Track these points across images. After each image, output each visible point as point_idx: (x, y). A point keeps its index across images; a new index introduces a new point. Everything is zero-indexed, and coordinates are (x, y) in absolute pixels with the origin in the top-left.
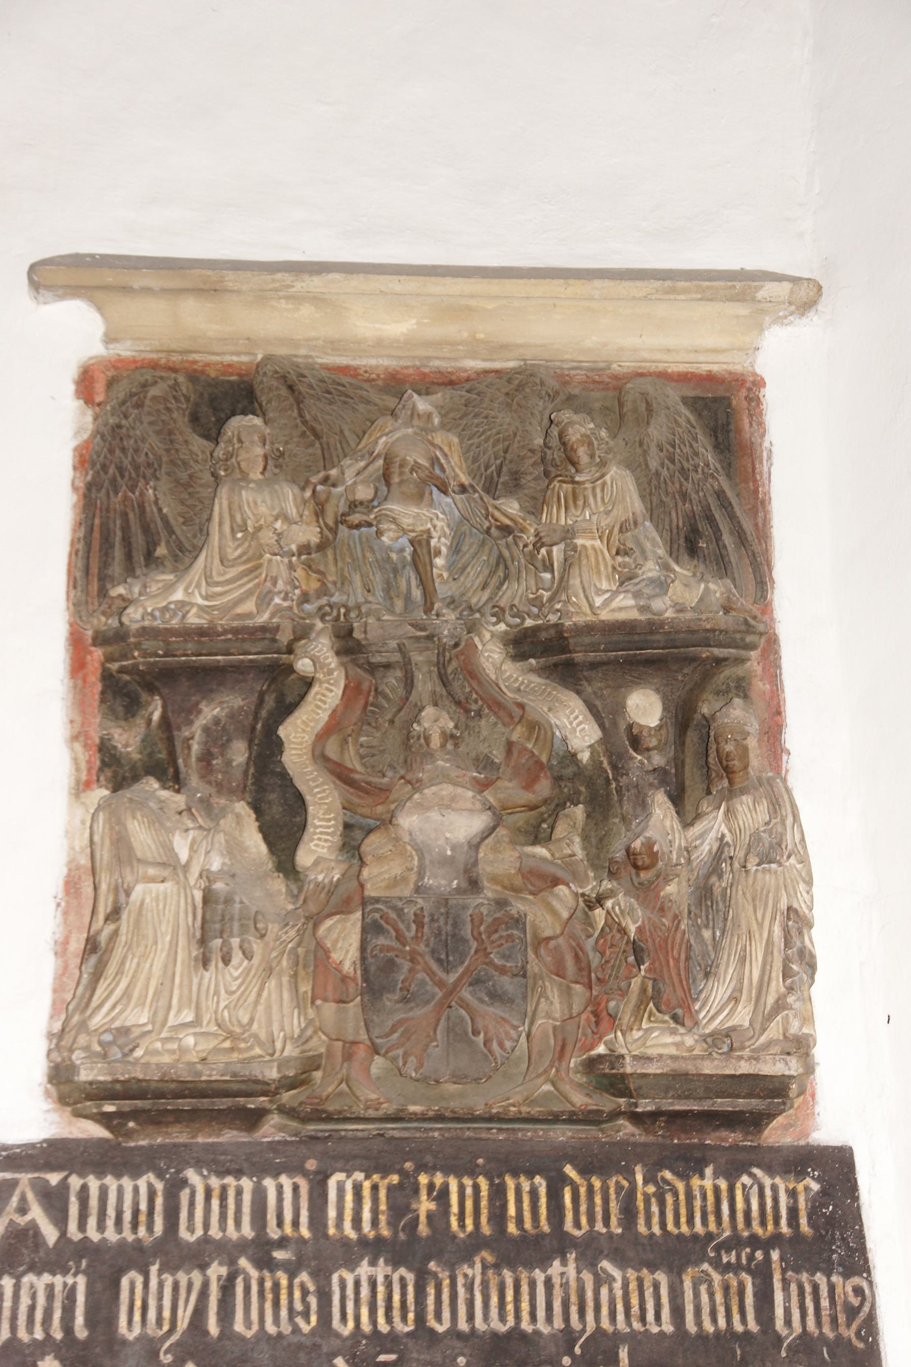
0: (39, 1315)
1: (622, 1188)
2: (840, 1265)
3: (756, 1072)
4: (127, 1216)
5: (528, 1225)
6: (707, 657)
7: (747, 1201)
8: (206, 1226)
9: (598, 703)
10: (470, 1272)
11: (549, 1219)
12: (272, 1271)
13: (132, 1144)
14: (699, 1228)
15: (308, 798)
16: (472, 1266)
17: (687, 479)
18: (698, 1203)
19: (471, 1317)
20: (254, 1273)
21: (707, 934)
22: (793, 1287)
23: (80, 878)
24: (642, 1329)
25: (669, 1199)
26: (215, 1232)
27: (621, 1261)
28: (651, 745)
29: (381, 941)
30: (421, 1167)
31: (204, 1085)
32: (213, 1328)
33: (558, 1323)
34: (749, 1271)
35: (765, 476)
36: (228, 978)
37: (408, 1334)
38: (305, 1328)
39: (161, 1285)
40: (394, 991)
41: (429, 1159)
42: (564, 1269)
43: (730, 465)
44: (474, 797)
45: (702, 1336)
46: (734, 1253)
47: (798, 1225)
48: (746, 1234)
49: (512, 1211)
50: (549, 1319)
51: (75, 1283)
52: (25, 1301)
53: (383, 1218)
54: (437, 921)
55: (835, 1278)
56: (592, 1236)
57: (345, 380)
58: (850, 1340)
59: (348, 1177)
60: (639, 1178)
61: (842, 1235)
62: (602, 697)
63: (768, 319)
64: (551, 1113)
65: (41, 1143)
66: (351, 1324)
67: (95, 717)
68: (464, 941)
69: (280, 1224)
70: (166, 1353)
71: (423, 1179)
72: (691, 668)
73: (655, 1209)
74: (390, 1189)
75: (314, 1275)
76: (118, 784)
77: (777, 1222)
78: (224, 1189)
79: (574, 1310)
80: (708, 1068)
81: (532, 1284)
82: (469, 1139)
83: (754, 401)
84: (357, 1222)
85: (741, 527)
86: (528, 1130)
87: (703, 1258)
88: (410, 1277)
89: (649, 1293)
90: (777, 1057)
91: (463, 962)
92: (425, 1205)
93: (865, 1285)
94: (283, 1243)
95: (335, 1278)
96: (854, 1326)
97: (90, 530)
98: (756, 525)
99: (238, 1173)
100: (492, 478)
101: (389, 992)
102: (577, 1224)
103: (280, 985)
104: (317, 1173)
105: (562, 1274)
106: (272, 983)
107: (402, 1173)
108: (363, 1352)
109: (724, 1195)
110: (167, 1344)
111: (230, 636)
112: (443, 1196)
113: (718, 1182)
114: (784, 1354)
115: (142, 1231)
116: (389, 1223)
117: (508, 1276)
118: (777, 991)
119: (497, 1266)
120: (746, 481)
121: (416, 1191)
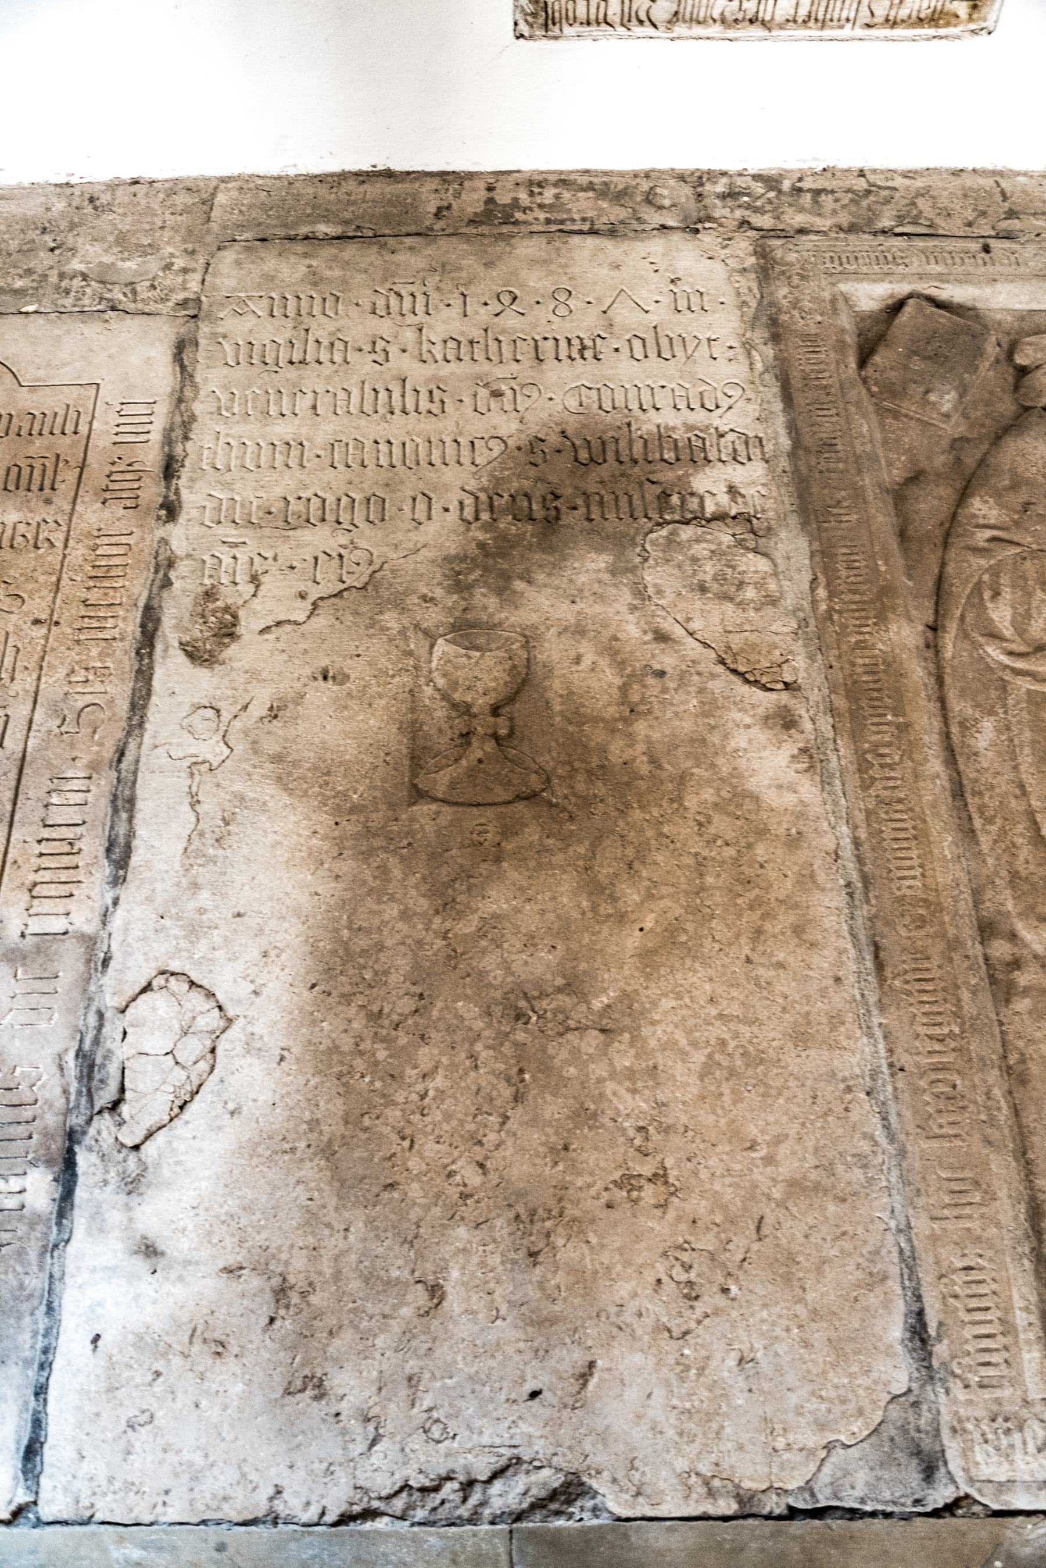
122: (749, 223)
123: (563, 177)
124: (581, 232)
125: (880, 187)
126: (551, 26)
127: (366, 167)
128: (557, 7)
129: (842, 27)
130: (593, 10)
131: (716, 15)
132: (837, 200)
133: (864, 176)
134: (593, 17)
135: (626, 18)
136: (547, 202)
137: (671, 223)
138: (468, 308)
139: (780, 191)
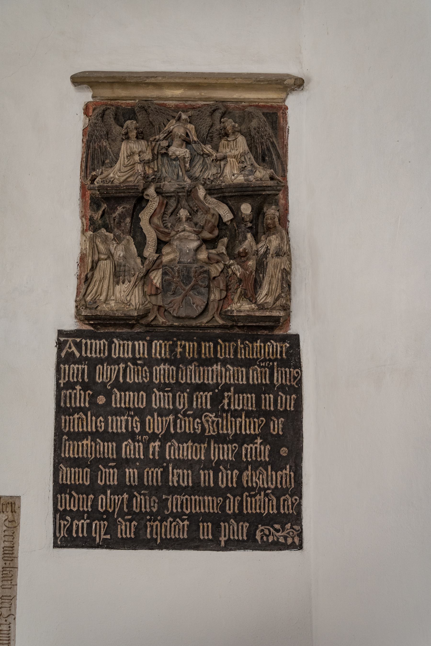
0: (75, 375)
1: (234, 345)
2: (293, 366)
3: (271, 315)
4: (98, 351)
5: (207, 355)
6: (265, 194)
7: (269, 349)
8: (119, 354)
9: (233, 207)
10: (191, 368)
11: (213, 354)
12: (137, 366)
13: (99, 332)
14: (255, 356)
15: (147, 236)
16: (191, 366)
17: (263, 139)
18: (255, 350)
19: (191, 379)
20: (132, 367)
21: (261, 275)
22: (280, 372)
23: (84, 257)
24: (238, 383)
25: (247, 349)
27: (233, 365)
28: (247, 220)
29: (167, 277)
30: (178, 339)
31: (117, 317)
32: (121, 380)
33: (215, 381)
34: (268, 367)
35: (287, 137)
36: (124, 287)
37: (174, 383)
38: (146, 381)
39: (107, 369)
40: (170, 292)
41: (180, 337)
42: (217, 367)
43: (276, 133)
44: (194, 236)
45: (254, 384)
46: (264, 363)
47: (282, 355)
48: (268, 358)
49: (203, 351)
50: (212, 380)
52: (71, 371)
53: (167, 353)
54: (183, 271)
55: (291, 370)
56: (225, 358)
57: (162, 108)
58: (294, 385)
59: (158, 342)
60: (239, 343)
61: (294, 358)
62: (234, 206)
63: (289, 89)
64: (214, 326)
65: (74, 330)
66: (158, 381)
67: (88, 210)
68: (191, 277)
69: (139, 354)
70: (109, 386)
71: (179, 343)
72: (260, 197)
73: (243, 351)
74: (169, 345)
75: (148, 367)
76: (95, 230)
77: (277, 355)
78: (124, 344)
79: (219, 378)
80: (258, 314)
81: (208, 371)
82: (192, 332)
83: (285, 114)
84: (160, 354)
85: (278, 153)
86: (208, 330)
87: (256, 364)
88: (175, 369)
89: (240, 374)
90: (277, 311)
91: (190, 284)
92: (179, 350)
93: (299, 371)
94: (140, 359)
95: (154, 368)
96: (295, 382)
97: (87, 155)
98: (283, 152)
99: (128, 340)
100: (205, 138)
101: (169, 291)
102: (221, 355)
103: (139, 289)
104: (149, 340)
105: (216, 368)
106: (136, 289)
107: (173, 341)
108: (161, 387)
109: (263, 347)
110: (109, 384)
111: (125, 188)
112: (185, 346)
113: (261, 344)
114: (276, 389)
115: (102, 355)
116: (169, 354)
117: (202, 369)
118: (279, 292)
119: (199, 366)
120: (281, 139)
121: (177, 346)
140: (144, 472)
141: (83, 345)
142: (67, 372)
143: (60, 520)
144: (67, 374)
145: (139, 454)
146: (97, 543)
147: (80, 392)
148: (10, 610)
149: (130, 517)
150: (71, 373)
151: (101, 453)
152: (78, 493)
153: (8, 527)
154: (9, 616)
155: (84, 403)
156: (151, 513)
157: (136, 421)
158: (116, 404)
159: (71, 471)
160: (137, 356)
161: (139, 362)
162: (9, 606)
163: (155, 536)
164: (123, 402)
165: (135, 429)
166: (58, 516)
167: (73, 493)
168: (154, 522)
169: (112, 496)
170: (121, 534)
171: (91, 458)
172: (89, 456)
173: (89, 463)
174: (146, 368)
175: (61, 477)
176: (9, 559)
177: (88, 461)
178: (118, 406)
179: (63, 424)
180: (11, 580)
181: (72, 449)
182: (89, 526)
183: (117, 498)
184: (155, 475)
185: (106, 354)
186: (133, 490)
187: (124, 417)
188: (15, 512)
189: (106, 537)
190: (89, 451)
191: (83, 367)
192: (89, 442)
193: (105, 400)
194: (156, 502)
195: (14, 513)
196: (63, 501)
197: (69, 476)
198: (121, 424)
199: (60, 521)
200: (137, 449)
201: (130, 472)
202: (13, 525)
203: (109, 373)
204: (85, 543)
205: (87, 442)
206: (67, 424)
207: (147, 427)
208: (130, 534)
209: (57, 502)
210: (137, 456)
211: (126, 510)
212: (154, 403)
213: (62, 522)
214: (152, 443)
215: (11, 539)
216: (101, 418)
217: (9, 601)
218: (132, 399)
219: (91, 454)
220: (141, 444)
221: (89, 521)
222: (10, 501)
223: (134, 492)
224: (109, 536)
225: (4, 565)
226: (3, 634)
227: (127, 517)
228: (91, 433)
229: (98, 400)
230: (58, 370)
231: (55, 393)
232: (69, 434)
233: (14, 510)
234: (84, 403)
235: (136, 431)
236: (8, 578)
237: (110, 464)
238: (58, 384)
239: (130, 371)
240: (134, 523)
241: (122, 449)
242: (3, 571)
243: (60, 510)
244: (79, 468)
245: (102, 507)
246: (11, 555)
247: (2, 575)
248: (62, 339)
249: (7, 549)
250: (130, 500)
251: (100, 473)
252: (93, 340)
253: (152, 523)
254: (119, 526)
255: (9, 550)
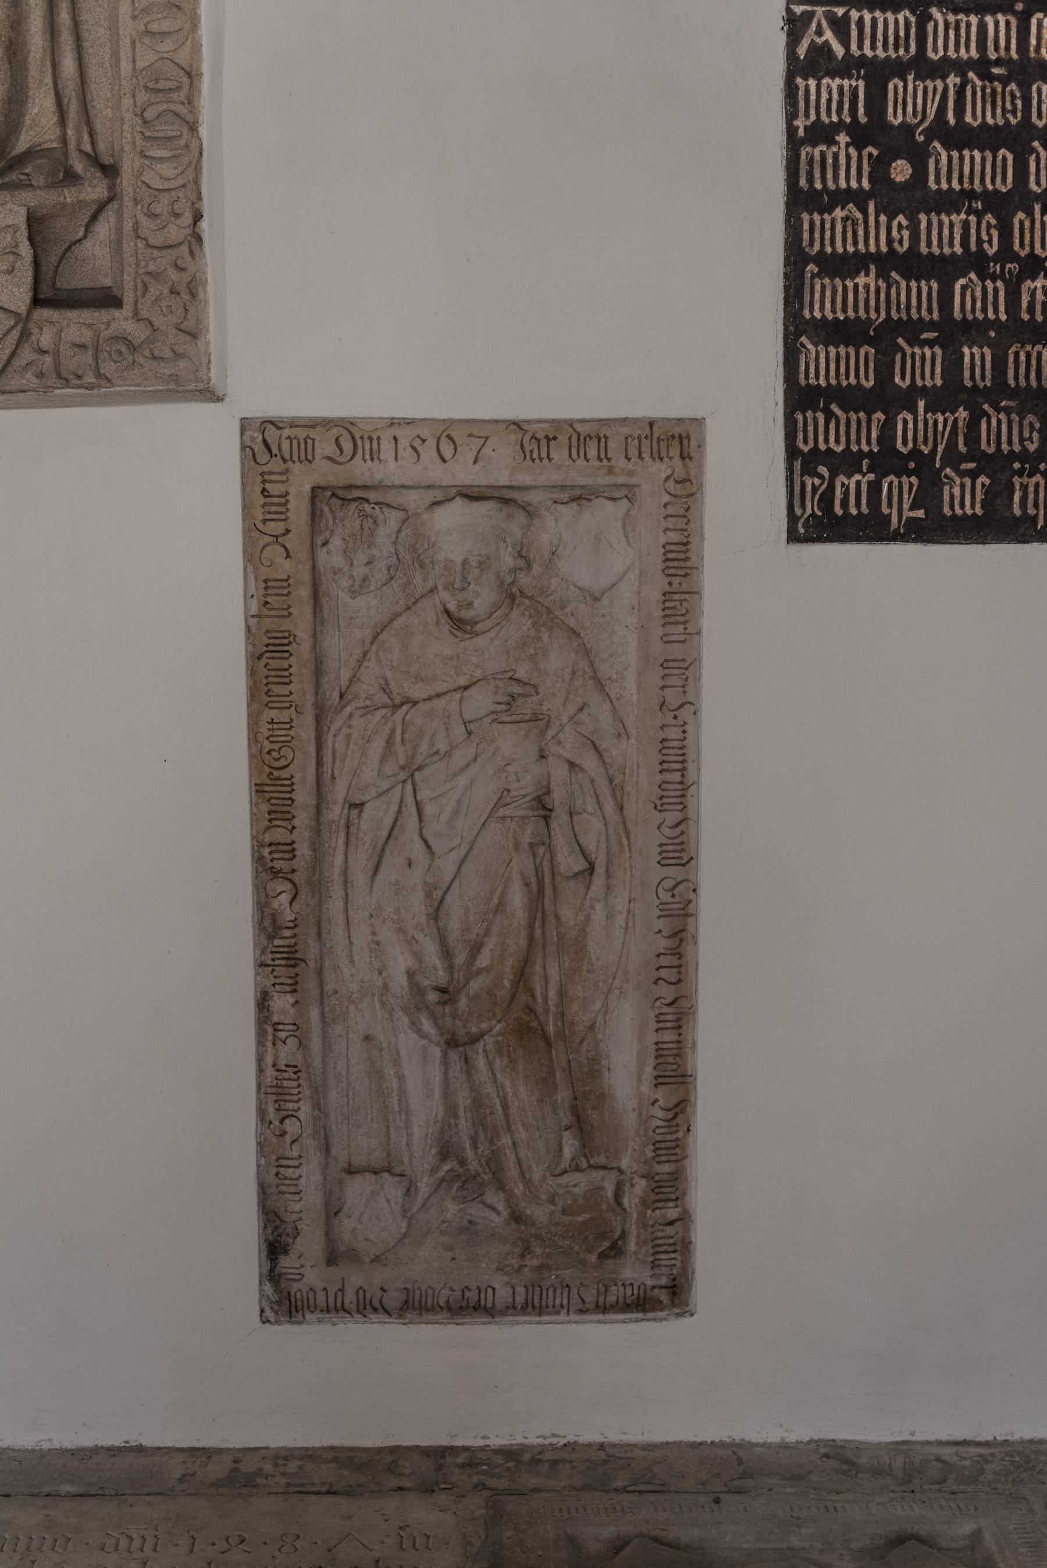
4: (891, 40)
8: (946, 48)
12: (991, 82)
20: (979, 83)
26: (952, 53)
38: (1013, 121)
51: (857, 86)
52: (824, 96)
69: (997, 49)
70: (920, 134)
75: (1020, 85)
78: (958, 23)
94: (998, 62)
95: (1034, 88)
99: (967, 12)
104: (1023, 12)
110: (921, 129)
115: (902, 51)
122: (484, 1485)
123: (310, 1453)
124: (319, 1493)
125: (618, 1458)
126: (294, 1313)
127: (118, 1442)
128: (299, 1296)
129: (558, 1313)
130: (331, 1300)
131: (442, 1302)
132: (573, 1468)
133: (604, 1450)
134: (331, 1305)
135: (361, 1308)
136: (289, 1471)
137: (407, 1485)
138: (196, 1547)
139: (519, 1462)
140: (1007, 355)
141: (853, 26)
142: (813, 97)
143: (802, 476)
144: (813, 104)
145: (996, 311)
146: (892, 529)
147: (846, 151)
148: (684, 692)
149: (972, 465)
150: (823, 100)
151: (902, 306)
152: (845, 409)
153: (675, 496)
154: (682, 706)
155: (859, 180)
156: (1024, 456)
157: (989, 226)
158: (938, 181)
159: (827, 353)
160: (993, 56)
161: (996, 71)
162: (681, 683)
163: (1031, 511)
164: (955, 175)
165: (986, 246)
166: (798, 465)
167: (835, 408)
168: (1030, 476)
169: (930, 414)
170: (952, 507)
171: (876, 320)
172: (873, 315)
173: (872, 333)
174: (1013, 86)
175: (803, 368)
176: (679, 572)
177: (871, 327)
178: (945, 186)
179: (806, 236)
180: (685, 622)
181: (830, 299)
182: (875, 488)
183: (941, 418)
184: (1034, 362)
185: (913, 49)
186: (980, 400)
187: (959, 215)
188: (691, 458)
189: (914, 515)
190: (872, 303)
191: (854, 84)
192: (871, 280)
193: (910, 171)
194: (1035, 429)
195: (687, 461)
196: (811, 428)
197: (822, 365)
198: (951, 233)
199: (804, 479)
200: (990, 298)
201: (972, 355)
202: (686, 489)
203: (920, 101)
204: (865, 530)
205: (867, 280)
206: (817, 235)
207: (1017, 241)
208: (973, 507)
209: (796, 432)
210: (991, 315)
211: (962, 447)
212: (1032, 178)
213: (809, 481)
214: (1029, 281)
215: (681, 523)
216: (901, 218)
217: (683, 671)
218: (978, 168)
219: (877, 310)
220: (999, 284)
221: (873, 475)
222: (677, 430)
223: (984, 404)
224: (923, 511)
225: (667, 588)
226: (669, 748)
227: (964, 466)
228: (877, 258)
229: (892, 171)
230: (790, 92)
231: (785, 154)
232: (821, 259)
233: (689, 453)
234: (859, 180)
235: (989, 252)
236: (677, 618)
237: (924, 336)
238: (791, 131)
239: (974, 94)
240: (983, 479)
241: (953, 297)
242: (664, 602)
243: (802, 451)
244: (847, 346)
245: (905, 442)
246: (682, 564)
247: (663, 610)
248: (798, 9)
249: (672, 548)
250: (973, 425)
251: (898, 357)
252: (878, 12)
253: (1025, 480)
254: (946, 488)
255: (679, 552)
